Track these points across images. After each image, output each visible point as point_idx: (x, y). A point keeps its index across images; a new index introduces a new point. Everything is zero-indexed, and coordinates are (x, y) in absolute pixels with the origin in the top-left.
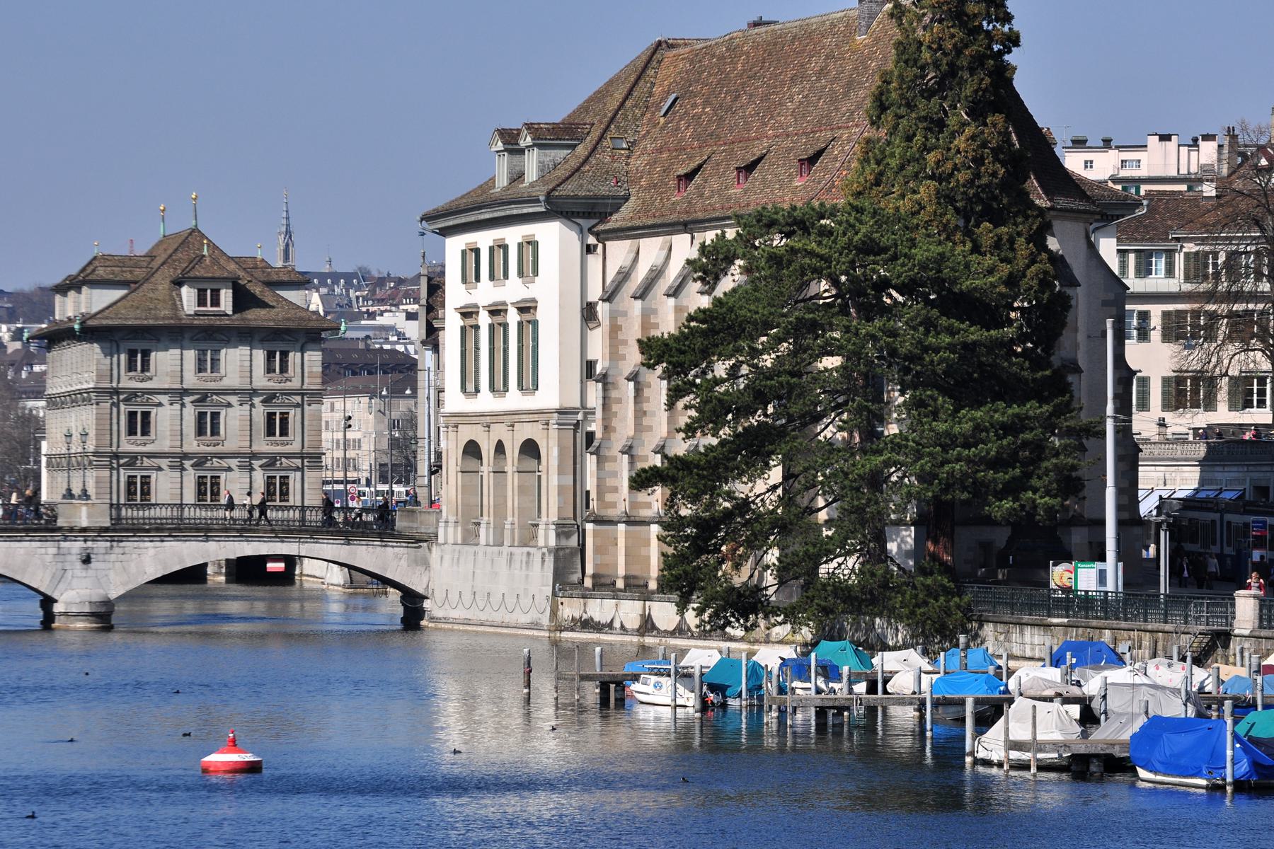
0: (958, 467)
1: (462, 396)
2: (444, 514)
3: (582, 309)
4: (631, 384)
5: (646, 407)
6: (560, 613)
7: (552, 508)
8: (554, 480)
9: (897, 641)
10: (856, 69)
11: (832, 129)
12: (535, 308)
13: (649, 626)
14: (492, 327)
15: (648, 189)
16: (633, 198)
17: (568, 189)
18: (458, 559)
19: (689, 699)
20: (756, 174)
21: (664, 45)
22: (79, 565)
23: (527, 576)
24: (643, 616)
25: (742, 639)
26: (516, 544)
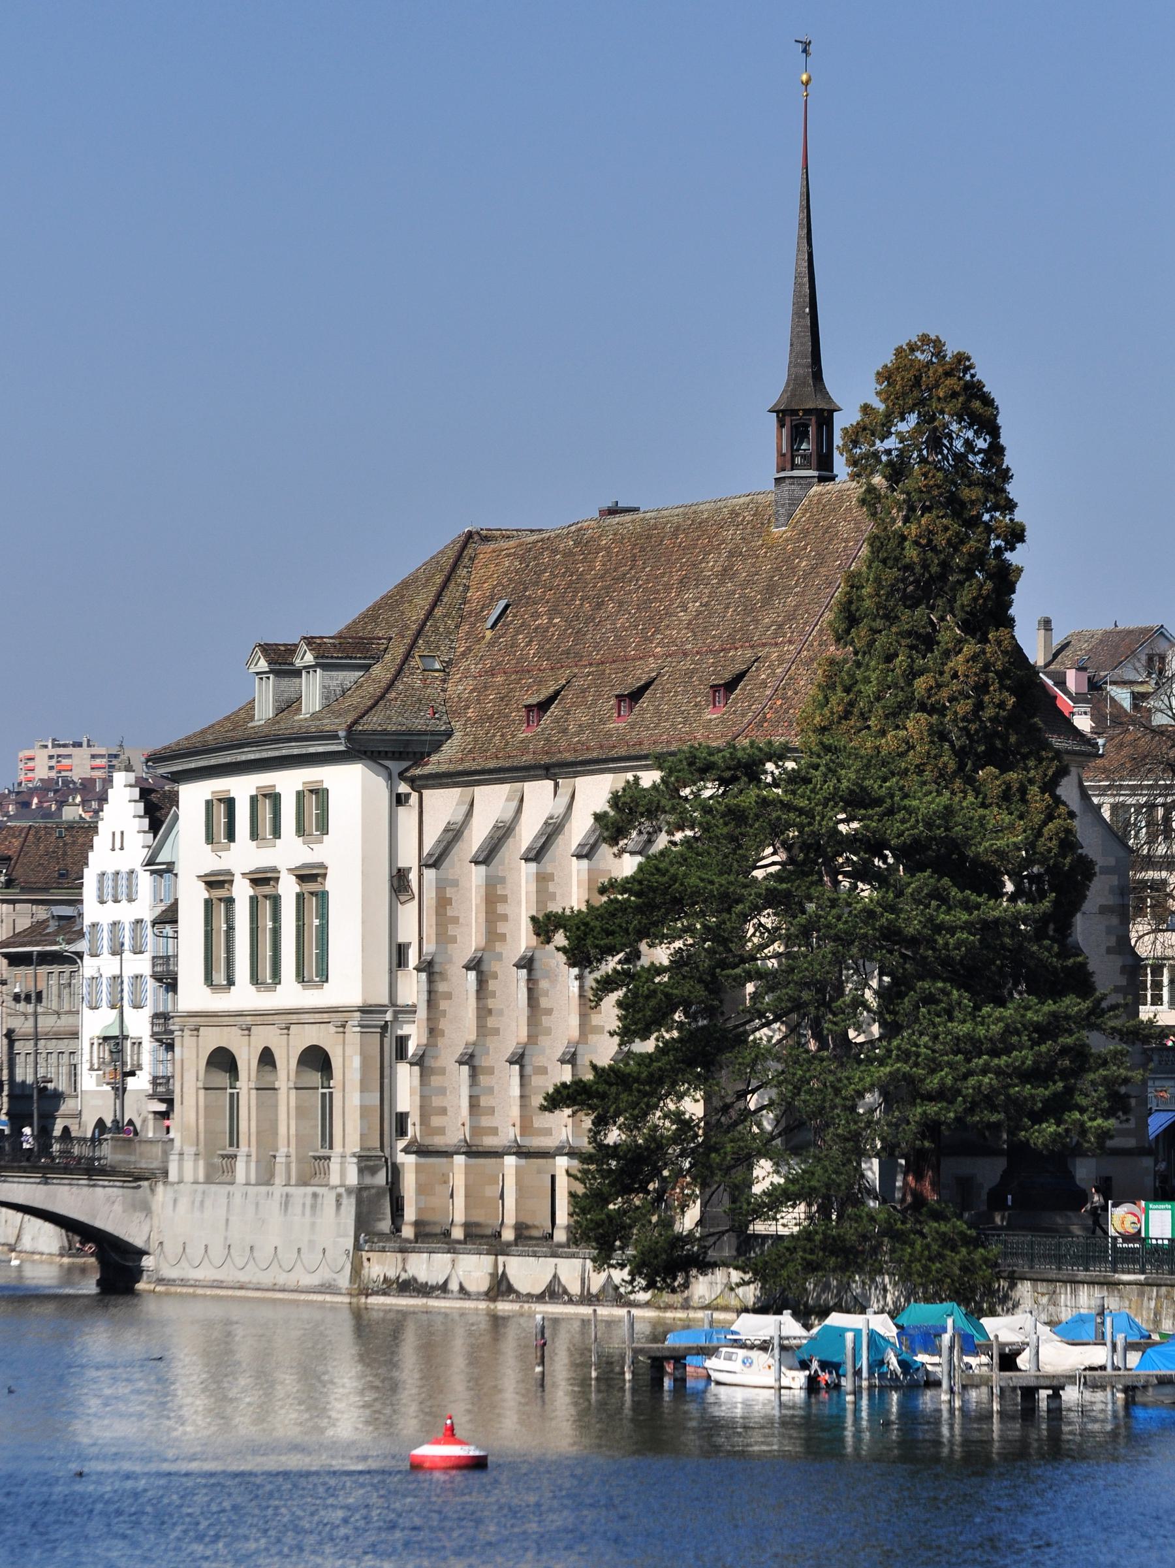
0: (987, 1080)
1: (208, 990)
2: (177, 1144)
3: (392, 877)
4: (472, 975)
5: (491, 1003)
6: (365, 1272)
9: (886, 1304)
10: (778, 569)
11: (752, 647)
12: (325, 875)
13: (504, 1287)
14: (254, 901)
15: (480, 721)
16: (457, 735)
17: (373, 722)
18: (202, 1202)
19: (797, 1380)
20: (644, 702)
21: (476, 538)
23: (313, 1224)
24: (494, 1275)
25: (647, 1304)
26: (293, 1182)
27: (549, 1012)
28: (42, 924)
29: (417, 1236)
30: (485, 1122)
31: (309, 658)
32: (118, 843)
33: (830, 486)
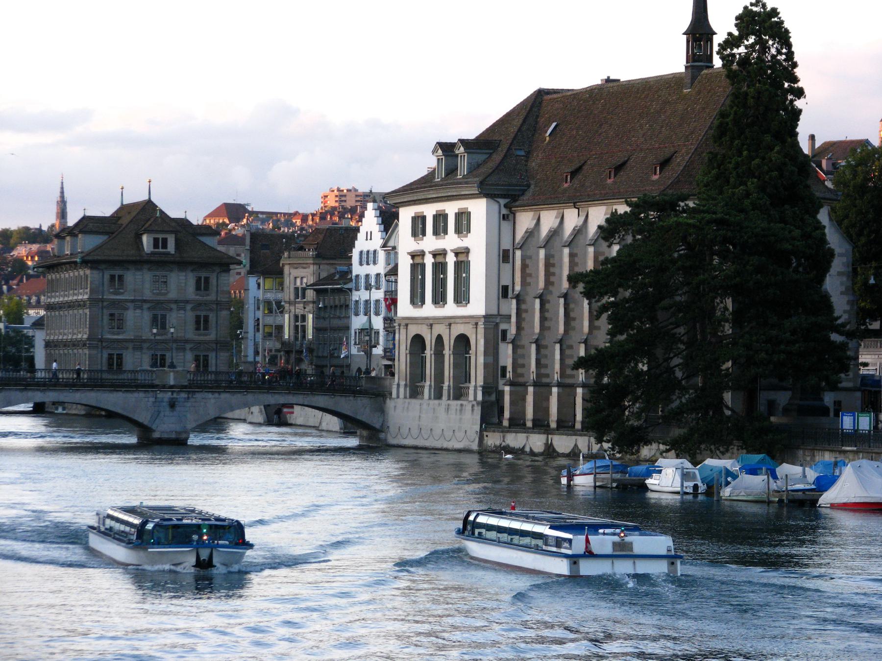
1: (411, 307)
4: (538, 301)
5: (547, 315)
6: (485, 442)
7: (478, 376)
8: (481, 360)
13: (551, 450)
16: (532, 186)
22: (168, 409)
23: (461, 419)
27: (574, 319)
28: (334, 275)
29: (510, 425)
30: (543, 371)
31: (462, 149)
32: (369, 236)
33: (710, 71)
